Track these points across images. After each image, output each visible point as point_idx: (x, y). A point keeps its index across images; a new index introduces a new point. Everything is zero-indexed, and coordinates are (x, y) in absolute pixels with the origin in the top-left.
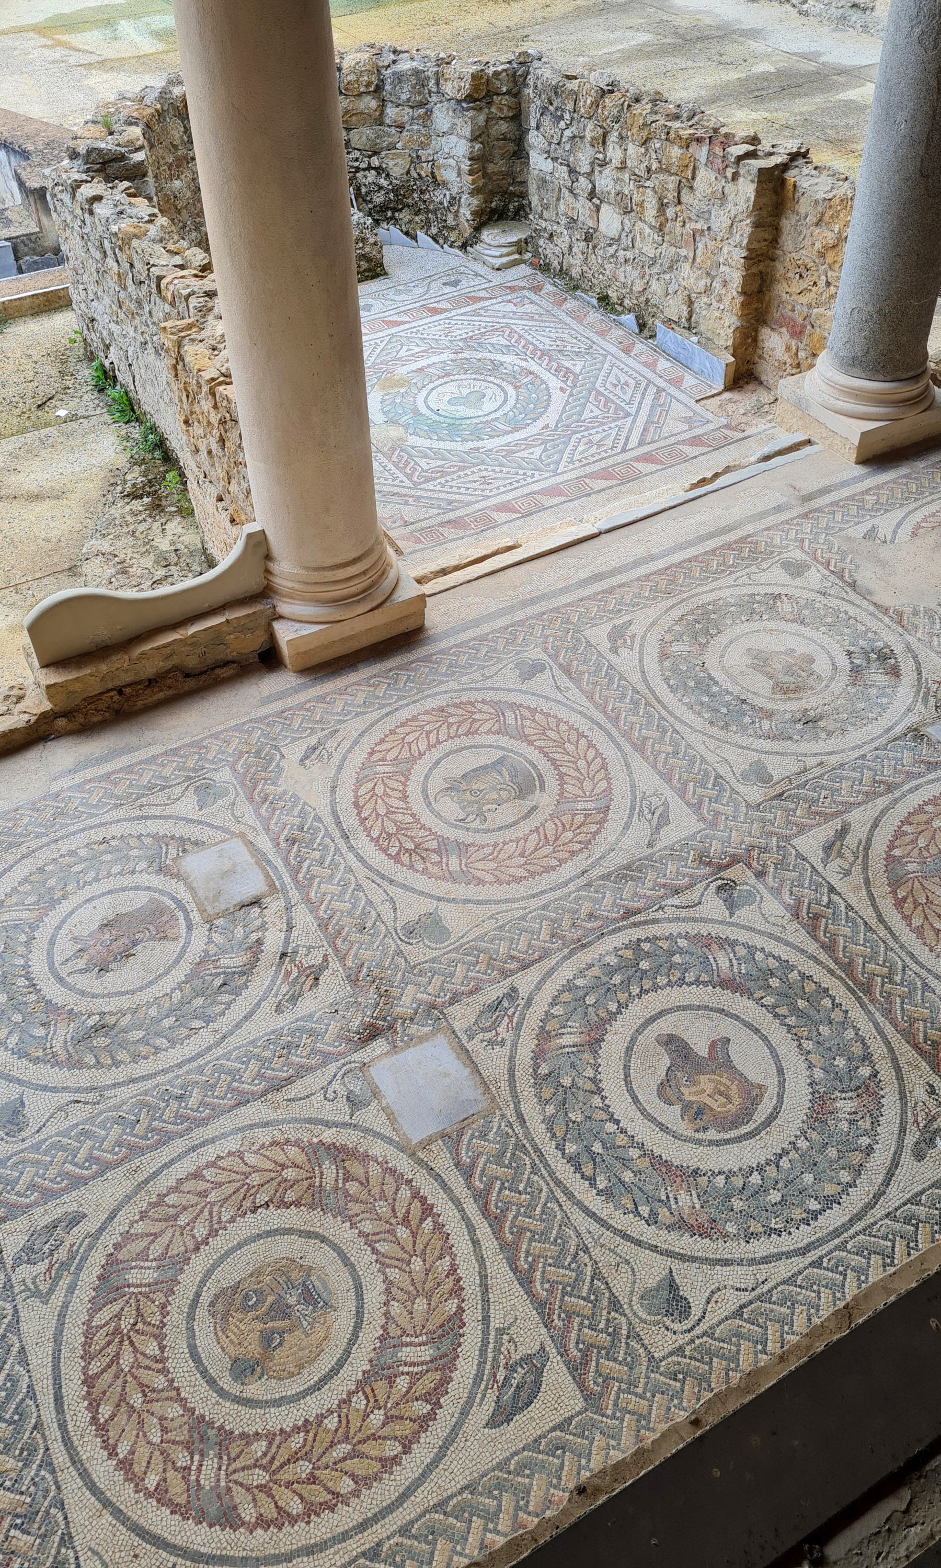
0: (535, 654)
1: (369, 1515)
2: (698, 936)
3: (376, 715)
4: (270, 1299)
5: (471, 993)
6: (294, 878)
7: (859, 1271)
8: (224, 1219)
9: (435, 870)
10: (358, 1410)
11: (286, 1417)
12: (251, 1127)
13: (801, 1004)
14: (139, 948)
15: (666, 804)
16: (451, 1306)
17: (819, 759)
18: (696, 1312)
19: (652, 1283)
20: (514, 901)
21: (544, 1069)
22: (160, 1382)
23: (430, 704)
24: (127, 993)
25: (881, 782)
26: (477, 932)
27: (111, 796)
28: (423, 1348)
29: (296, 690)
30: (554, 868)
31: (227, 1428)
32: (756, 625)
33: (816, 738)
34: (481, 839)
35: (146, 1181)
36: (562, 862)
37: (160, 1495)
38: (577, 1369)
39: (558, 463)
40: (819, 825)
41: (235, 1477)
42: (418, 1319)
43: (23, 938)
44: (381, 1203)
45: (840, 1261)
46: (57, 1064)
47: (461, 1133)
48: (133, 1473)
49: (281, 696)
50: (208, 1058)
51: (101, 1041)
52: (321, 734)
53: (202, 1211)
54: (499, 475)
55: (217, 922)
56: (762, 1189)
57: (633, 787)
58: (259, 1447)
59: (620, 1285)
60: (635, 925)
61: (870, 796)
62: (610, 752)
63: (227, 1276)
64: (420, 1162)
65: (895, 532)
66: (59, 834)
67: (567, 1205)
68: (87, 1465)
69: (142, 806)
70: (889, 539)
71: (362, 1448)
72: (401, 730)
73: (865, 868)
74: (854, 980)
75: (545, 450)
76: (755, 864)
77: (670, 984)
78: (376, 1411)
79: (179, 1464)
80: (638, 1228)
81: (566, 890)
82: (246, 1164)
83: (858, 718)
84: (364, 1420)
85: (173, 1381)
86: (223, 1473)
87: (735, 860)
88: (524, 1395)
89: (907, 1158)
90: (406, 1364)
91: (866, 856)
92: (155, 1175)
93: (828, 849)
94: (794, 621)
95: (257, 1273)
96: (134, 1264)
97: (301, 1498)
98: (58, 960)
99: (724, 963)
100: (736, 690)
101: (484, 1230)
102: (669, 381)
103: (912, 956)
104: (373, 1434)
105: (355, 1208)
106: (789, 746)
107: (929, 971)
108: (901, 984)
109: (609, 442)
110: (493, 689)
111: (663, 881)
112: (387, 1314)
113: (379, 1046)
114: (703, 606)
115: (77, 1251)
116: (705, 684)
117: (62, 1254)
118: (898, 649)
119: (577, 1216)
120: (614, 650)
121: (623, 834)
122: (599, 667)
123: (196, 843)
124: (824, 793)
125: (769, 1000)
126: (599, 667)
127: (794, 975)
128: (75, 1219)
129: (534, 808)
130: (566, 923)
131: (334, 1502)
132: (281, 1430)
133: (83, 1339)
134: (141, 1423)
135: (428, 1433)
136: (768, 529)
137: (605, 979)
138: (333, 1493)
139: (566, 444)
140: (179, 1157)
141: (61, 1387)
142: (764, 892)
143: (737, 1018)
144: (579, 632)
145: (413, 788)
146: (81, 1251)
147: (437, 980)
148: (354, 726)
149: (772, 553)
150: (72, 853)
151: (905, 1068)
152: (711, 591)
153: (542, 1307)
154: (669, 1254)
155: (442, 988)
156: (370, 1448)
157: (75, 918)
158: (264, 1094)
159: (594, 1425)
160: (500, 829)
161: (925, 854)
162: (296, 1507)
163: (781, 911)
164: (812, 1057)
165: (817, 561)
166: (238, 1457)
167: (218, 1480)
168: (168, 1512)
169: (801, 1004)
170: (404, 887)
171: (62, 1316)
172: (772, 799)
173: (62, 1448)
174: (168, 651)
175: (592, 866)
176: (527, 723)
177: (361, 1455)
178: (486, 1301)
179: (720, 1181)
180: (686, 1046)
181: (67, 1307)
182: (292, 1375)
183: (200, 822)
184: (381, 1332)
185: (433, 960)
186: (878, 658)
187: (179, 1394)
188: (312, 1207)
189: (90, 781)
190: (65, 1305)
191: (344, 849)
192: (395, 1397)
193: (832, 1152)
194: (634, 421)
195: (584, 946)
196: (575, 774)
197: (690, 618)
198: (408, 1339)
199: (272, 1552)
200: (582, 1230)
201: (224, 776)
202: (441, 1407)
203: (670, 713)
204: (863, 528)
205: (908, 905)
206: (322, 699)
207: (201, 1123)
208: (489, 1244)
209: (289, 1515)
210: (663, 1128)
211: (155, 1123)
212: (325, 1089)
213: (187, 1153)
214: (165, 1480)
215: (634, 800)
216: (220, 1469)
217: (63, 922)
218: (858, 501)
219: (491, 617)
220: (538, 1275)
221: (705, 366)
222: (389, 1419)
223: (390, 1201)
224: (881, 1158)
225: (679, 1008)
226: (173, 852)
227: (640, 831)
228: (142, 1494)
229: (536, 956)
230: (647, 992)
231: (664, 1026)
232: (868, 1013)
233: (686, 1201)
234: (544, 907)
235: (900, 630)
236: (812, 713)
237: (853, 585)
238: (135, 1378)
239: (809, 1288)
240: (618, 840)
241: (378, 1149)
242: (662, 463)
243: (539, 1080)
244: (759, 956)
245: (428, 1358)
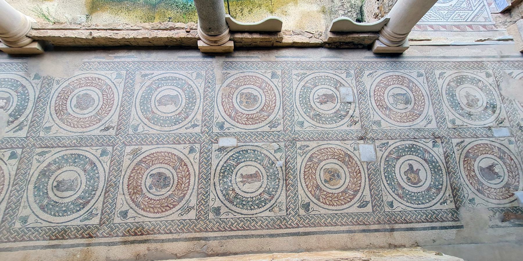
0: (423, 71)
2: (425, 149)
3: (385, 71)
4: (333, 173)
5: (381, 140)
6: (358, 101)
7: (422, 216)
9: (383, 112)
11: (330, 191)
12: (337, 145)
13: (436, 170)
14: (328, 102)
15: (432, 119)
16: (358, 188)
17: (466, 124)
18: (394, 208)
19: (389, 201)
20: (395, 125)
21: (387, 159)
22: (314, 177)
23: (397, 74)
24: (324, 110)
25: (476, 135)
26: (386, 128)
27: (331, 67)
29: (372, 58)
30: (405, 122)
32: (471, 86)
33: (469, 119)
34: (394, 109)
35: (319, 146)
36: (407, 122)
37: (311, 192)
38: (373, 207)
39: (449, 18)
40: (459, 138)
43: (310, 91)
45: (419, 212)
46: (310, 118)
47: (370, 163)
49: (369, 58)
50: (334, 129)
51: (318, 117)
52: (373, 71)
54: (434, 16)
55: (342, 104)
56: (413, 196)
57: (428, 112)
59: (384, 199)
60: (415, 141)
61: (472, 137)
62: (427, 102)
63: (327, 167)
64: (362, 164)
65: (516, 76)
66: (320, 71)
67: (382, 183)
69: (336, 72)
70: (514, 77)
72: (389, 77)
73: (462, 151)
74: (448, 171)
75: (448, 13)
76: (442, 140)
77: (415, 155)
80: (391, 192)
81: (405, 128)
83: (480, 118)
87: (439, 137)
88: (364, 206)
89: (439, 203)
91: (464, 149)
92: (321, 145)
93: (457, 144)
94: (480, 89)
95: (332, 168)
98: (315, 98)
99: (427, 156)
100: (459, 100)
101: (367, 180)
102: (488, 3)
103: (461, 171)
105: (349, 166)
106: (463, 119)
107: (462, 176)
108: (455, 176)
109: (464, 17)
110: (410, 76)
111: (424, 135)
113: (362, 141)
114: (463, 75)
116: (453, 96)
117: (305, 151)
118: (498, 107)
119: (382, 185)
120: (439, 78)
121: (421, 122)
122: (434, 81)
123: (343, 85)
124: (464, 132)
125: (431, 167)
126: (434, 81)
127: (438, 165)
128: (308, 146)
129: (407, 108)
130: (403, 134)
136: (488, 61)
137: (405, 149)
139: (454, 13)
140: (325, 144)
142: (441, 146)
143: (424, 167)
144: (434, 70)
145: (386, 92)
147: (376, 134)
148: (381, 72)
149: (486, 68)
150: (321, 76)
151: (447, 190)
152: (467, 72)
153: (371, 195)
154: (394, 198)
155: (376, 136)
157: (319, 91)
158: (341, 140)
159: (372, 215)
160: (399, 109)
161: (475, 154)
162: (328, 203)
163: (442, 152)
164: (433, 180)
165: (494, 76)
169: (436, 170)
170: (377, 113)
171: (303, 160)
172: (453, 128)
174: (354, 38)
175: (412, 125)
176: (414, 87)
177: (339, 201)
178: (364, 190)
179: (407, 191)
180: (413, 167)
183: (345, 81)
185: (377, 130)
186: (493, 107)
188: (343, 163)
189: (328, 61)
190: (304, 159)
191: (369, 100)
192: (346, 196)
193: (427, 196)
194: (473, 13)
195: (404, 140)
196: (418, 104)
197: (459, 77)
200: (382, 188)
201: (352, 72)
203: (443, 99)
204: (510, 71)
205: (466, 162)
206: (376, 62)
207: (330, 140)
208: (367, 182)
210: (402, 179)
211: (323, 137)
212: (351, 144)
213: (327, 144)
215: (426, 116)
217: (317, 90)
218: (513, 63)
219: (418, 57)
220: (373, 191)
221: (501, 3)
222: (344, 199)
224: (435, 201)
225: (415, 160)
226: (339, 85)
227: (424, 123)
229: (395, 138)
230: (411, 154)
231: (410, 162)
232: (447, 177)
233: (400, 192)
234: (400, 129)
235: (502, 102)
236: (471, 113)
237: (498, 86)
239: (413, 214)
240: (419, 123)
241: (356, 159)
242: (473, 30)
243: (386, 161)
244: (433, 158)
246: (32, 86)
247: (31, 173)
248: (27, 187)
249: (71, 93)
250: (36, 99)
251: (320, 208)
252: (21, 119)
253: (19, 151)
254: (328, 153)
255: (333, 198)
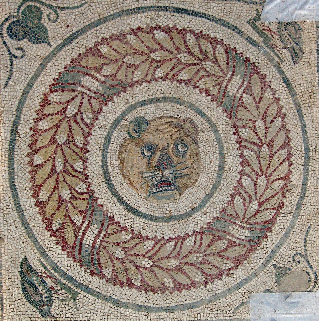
1: (15, 166)
4: (175, 159)
8: (245, 151)
10: (77, 185)
28: (92, 242)
31: (110, 103)
37: (94, 51)
41: (80, 97)
42: (111, 249)
44: (200, 259)
48: (115, 39)
53: (259, 138)
58: (88, 117)
68: (133, 16)
71: (54, 177)
78: (70, 196)
79: (105, 67)
82: (276, 180)
84: (69, 185)
85: (157, 81)
86: (86, 91)
90: (88, 226)
96: (246, 83)
97: (46, 131)
104: (58, 188)
105: (207, 239)
112: (125, 229)
115: (273, 51)
117: (276, 41)
131: (34, 149)
132: (91, 134)
133: (212, 36)
134: (142, 54)
135: (40, 221)
138: (38, 150)
141: (189, 14)
146: (272, 54)
156: (51, 183)
162: (43, 125)
166: (90, 103)
167: (83, 86)
168: (81, 52)
171: (234, 28)
173: (151, 5)
177: (50, 176)
181: (239, 33)
182: (120, 153)
184: (116, 220)
187: (146, 81)
190: (240, 33)
198: (102, 235)
199: (27, 103)
202: (51, 236)
209: (41, 119)
214: (101, 56)
216: (89, 90)
222: (61, 201)
223: (198, 265)
228: (99, 41)
238: (171, 59)
245: (84, 242)
251: (20, 88)
254: (265, 149)
255: (67, 151)
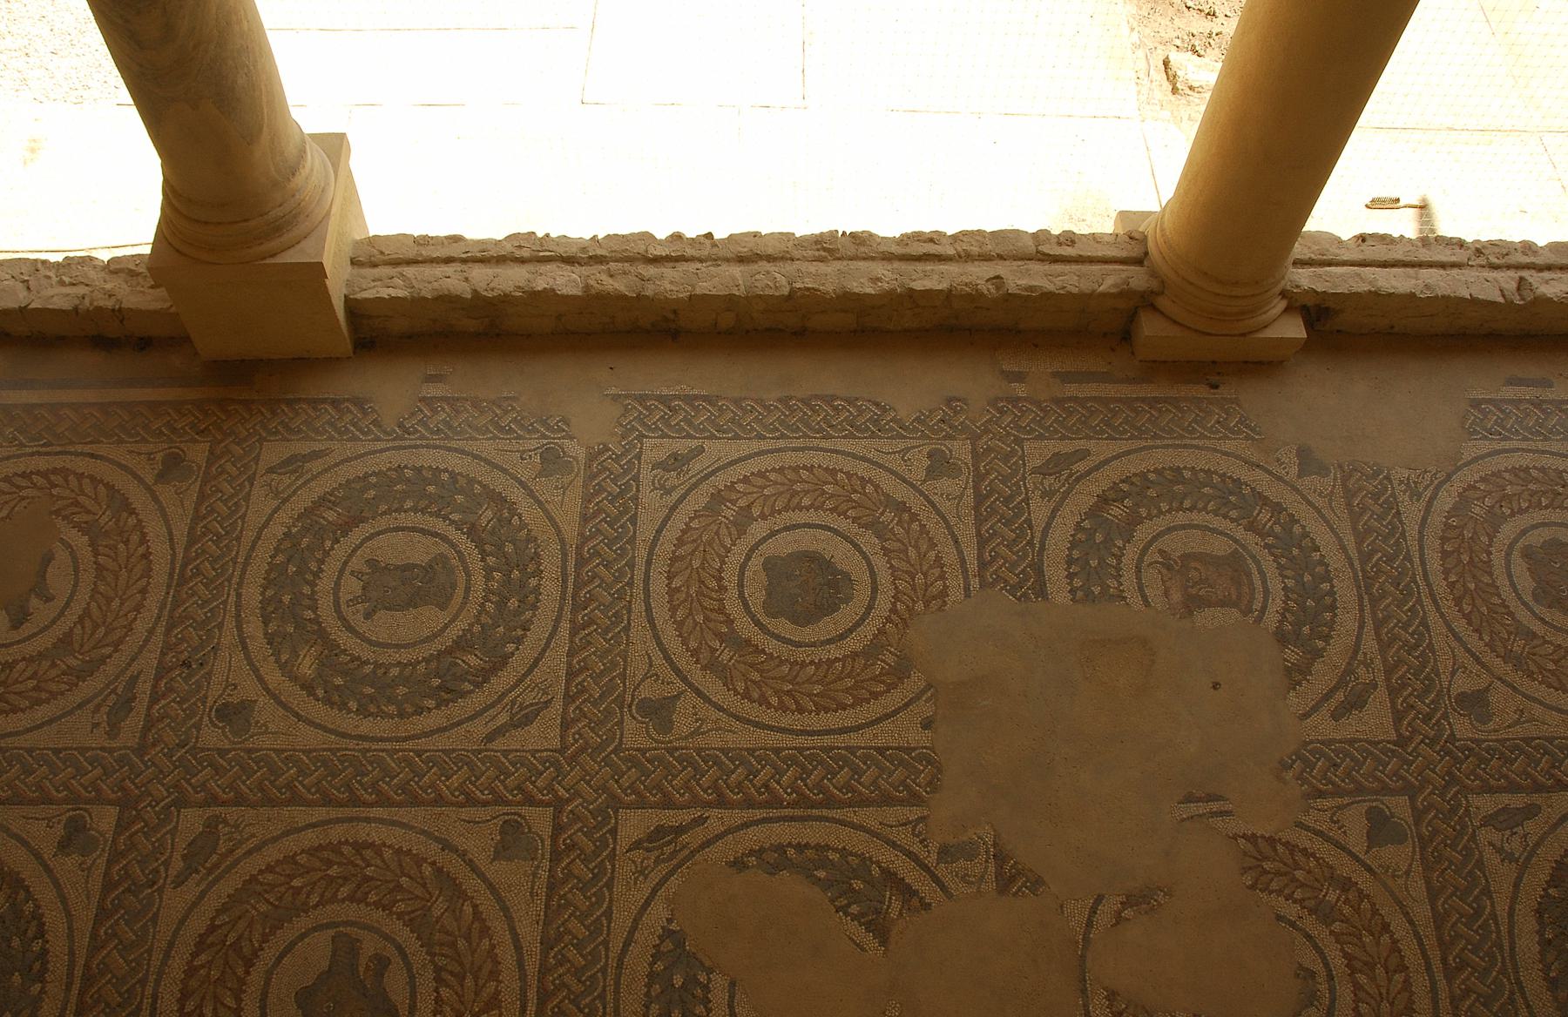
246: (1309, 503)
247: (1502, 914)
248: (1518, 982)
249: (1491, 540)
250: (1357, 564)
252: (1336, 651)
253: (1399, 806)
